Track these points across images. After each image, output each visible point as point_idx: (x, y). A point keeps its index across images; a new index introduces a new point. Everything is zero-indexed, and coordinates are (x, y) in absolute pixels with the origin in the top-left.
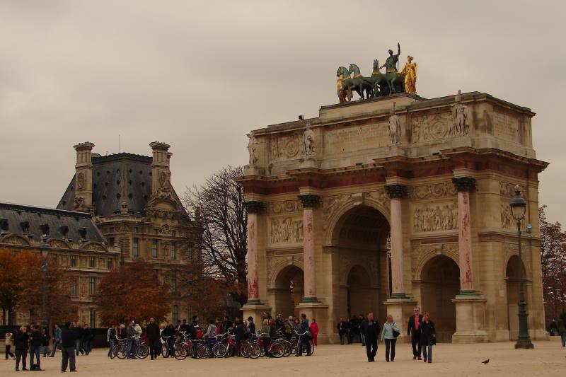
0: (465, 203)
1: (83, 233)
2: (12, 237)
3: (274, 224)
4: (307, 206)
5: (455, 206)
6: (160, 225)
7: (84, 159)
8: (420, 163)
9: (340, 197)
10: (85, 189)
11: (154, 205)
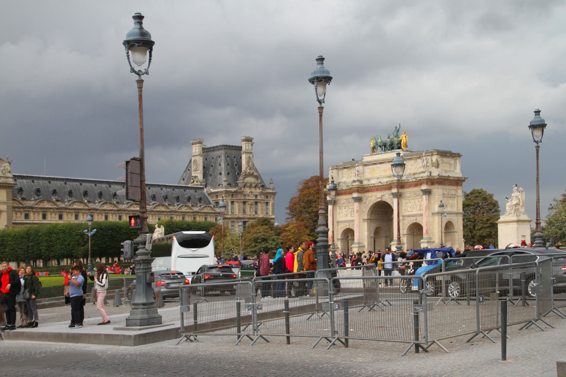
0: (426, 200)
1: (200, 200)
2: (159, 205)
3: (340, 209)
4: (356, 202)
5: (422, 201)
6: (247, 192)
7: (197, 150)
8: (407, 182)
9: (371, 197)
10: (198, 170)
11: (244, 179)
